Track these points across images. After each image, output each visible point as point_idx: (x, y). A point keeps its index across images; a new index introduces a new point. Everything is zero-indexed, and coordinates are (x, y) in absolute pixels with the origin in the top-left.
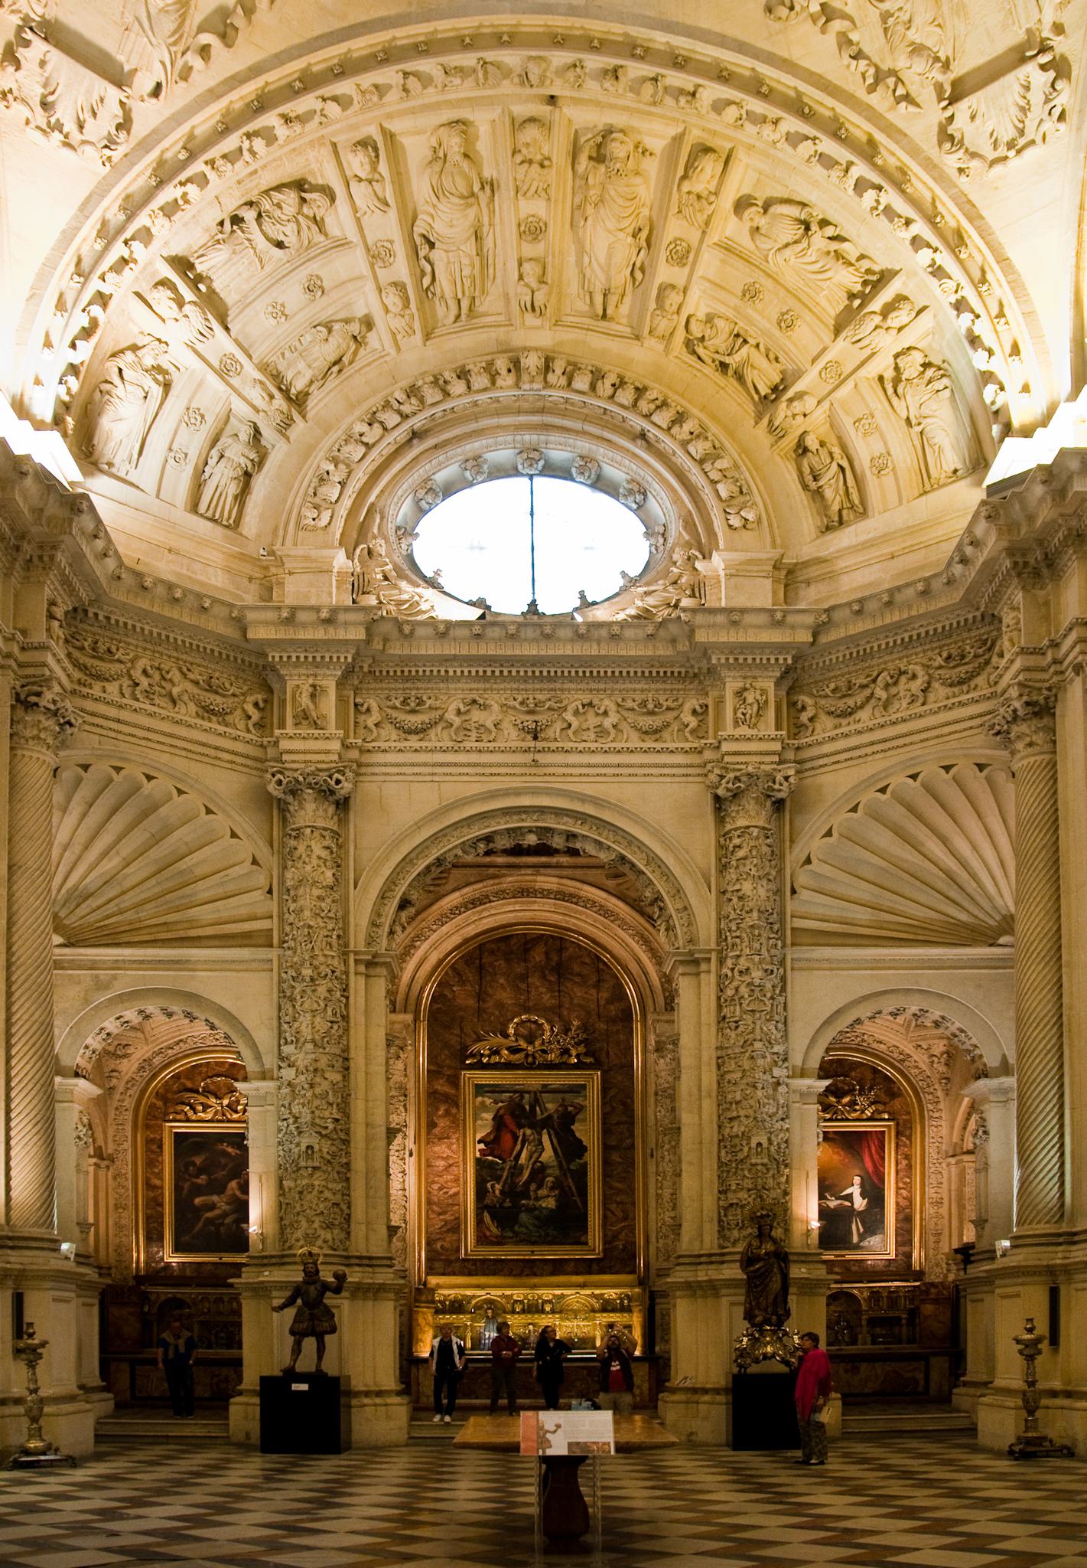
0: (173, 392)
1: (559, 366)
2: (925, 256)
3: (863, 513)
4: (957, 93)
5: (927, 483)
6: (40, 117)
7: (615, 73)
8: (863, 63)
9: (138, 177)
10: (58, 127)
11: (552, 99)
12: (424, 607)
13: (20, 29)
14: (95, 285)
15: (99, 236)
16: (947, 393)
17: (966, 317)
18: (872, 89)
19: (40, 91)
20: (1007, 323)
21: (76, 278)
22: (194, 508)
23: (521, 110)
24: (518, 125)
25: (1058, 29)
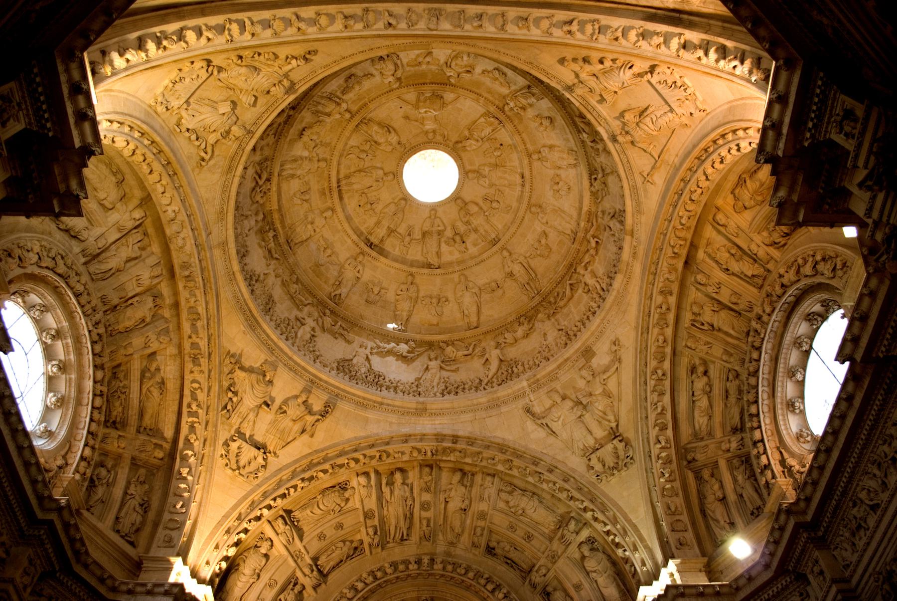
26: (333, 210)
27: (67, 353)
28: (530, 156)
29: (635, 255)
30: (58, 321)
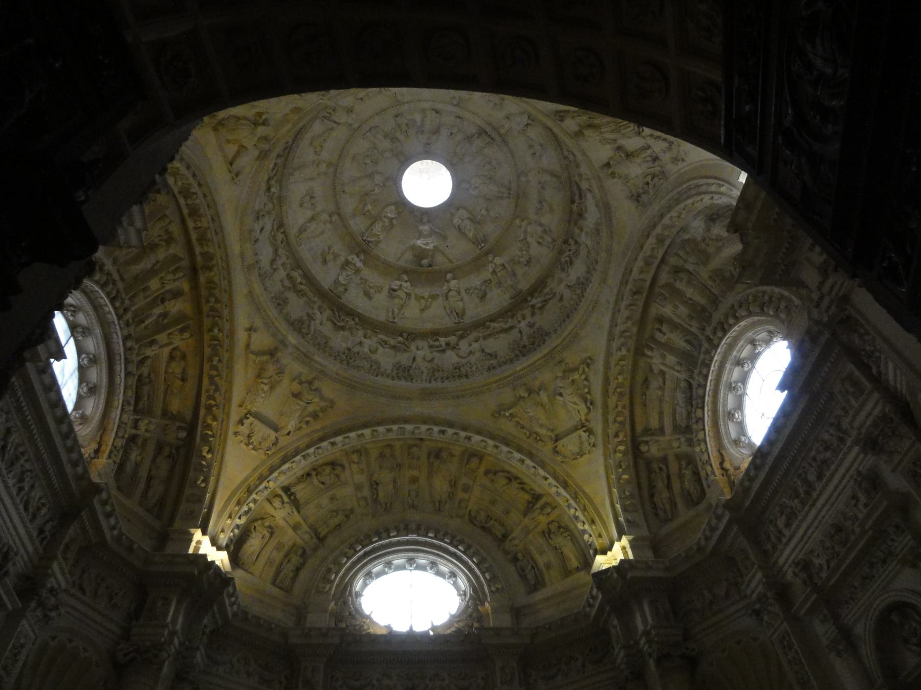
0: (274, 536)
1: (423, 528)
2: (554, 490)
3: (544, 585)
4: (557, 439)
5: (567, 572)
6: (246, 441)
7: (443, 432)
8: (525, 431)
9: (276, 460)
10: (252, 443)
11: (421, 439)
12: (365, 628)
13: (246, 414)
14: (254, 496)
15: (258, 479)
16: (569, 538)
17: (572, 511)
18: (529, 437)
19: (248, 432)
20: (588, 512)
21: (247, 493)
22: (274, 583)
23: (410, 442)
24: (410, 447)
25: (587, 420)
26: (519, 177)
27: (743, 348)
28: (339, 214)
29: (242, 255)
30: (731, 371)
